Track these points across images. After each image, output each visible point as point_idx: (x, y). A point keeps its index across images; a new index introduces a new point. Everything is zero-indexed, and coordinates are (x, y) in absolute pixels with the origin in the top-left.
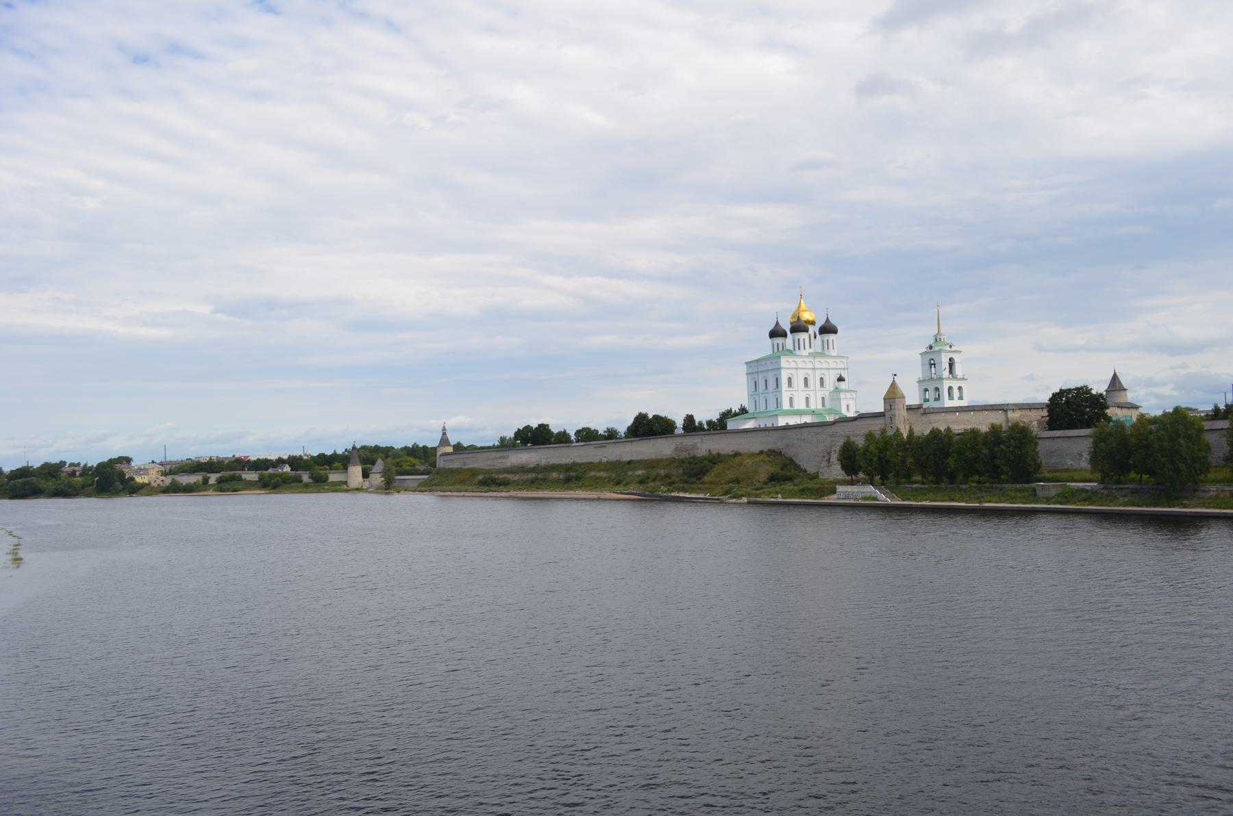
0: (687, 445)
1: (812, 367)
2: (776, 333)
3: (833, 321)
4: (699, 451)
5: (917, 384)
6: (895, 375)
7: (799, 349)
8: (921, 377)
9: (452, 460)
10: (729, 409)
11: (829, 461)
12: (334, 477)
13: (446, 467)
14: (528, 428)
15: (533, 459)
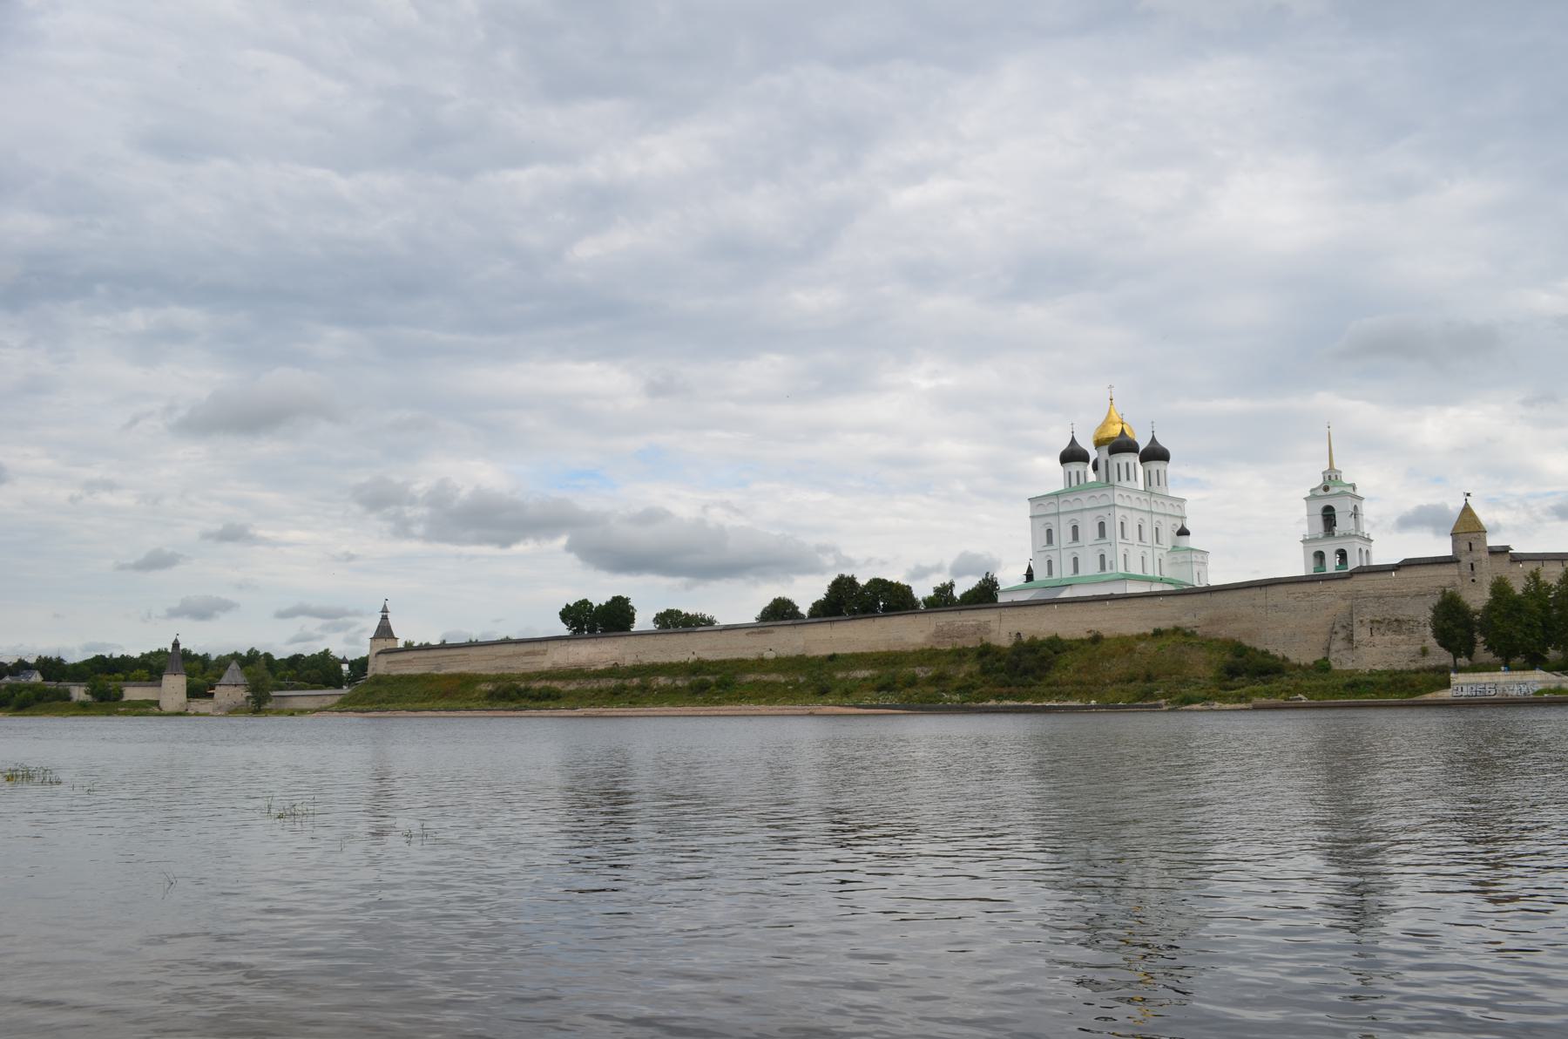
0: (962, 626)
1: (1147, 509)
2: (1072, 455)
3: (1163, 442)
4: (993, 635)
5: (1302, 544)
6: (1468, 495)
7: (1128, 479)
8: (1307, 534)
9: (409, 661)
10: (947, 582)
11: (1349, 639)
12: (133, 693)
13: (394, 673)
14: (584, 603)
15: (606, 656)
